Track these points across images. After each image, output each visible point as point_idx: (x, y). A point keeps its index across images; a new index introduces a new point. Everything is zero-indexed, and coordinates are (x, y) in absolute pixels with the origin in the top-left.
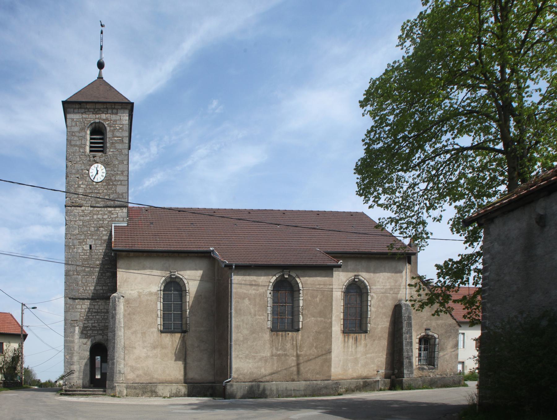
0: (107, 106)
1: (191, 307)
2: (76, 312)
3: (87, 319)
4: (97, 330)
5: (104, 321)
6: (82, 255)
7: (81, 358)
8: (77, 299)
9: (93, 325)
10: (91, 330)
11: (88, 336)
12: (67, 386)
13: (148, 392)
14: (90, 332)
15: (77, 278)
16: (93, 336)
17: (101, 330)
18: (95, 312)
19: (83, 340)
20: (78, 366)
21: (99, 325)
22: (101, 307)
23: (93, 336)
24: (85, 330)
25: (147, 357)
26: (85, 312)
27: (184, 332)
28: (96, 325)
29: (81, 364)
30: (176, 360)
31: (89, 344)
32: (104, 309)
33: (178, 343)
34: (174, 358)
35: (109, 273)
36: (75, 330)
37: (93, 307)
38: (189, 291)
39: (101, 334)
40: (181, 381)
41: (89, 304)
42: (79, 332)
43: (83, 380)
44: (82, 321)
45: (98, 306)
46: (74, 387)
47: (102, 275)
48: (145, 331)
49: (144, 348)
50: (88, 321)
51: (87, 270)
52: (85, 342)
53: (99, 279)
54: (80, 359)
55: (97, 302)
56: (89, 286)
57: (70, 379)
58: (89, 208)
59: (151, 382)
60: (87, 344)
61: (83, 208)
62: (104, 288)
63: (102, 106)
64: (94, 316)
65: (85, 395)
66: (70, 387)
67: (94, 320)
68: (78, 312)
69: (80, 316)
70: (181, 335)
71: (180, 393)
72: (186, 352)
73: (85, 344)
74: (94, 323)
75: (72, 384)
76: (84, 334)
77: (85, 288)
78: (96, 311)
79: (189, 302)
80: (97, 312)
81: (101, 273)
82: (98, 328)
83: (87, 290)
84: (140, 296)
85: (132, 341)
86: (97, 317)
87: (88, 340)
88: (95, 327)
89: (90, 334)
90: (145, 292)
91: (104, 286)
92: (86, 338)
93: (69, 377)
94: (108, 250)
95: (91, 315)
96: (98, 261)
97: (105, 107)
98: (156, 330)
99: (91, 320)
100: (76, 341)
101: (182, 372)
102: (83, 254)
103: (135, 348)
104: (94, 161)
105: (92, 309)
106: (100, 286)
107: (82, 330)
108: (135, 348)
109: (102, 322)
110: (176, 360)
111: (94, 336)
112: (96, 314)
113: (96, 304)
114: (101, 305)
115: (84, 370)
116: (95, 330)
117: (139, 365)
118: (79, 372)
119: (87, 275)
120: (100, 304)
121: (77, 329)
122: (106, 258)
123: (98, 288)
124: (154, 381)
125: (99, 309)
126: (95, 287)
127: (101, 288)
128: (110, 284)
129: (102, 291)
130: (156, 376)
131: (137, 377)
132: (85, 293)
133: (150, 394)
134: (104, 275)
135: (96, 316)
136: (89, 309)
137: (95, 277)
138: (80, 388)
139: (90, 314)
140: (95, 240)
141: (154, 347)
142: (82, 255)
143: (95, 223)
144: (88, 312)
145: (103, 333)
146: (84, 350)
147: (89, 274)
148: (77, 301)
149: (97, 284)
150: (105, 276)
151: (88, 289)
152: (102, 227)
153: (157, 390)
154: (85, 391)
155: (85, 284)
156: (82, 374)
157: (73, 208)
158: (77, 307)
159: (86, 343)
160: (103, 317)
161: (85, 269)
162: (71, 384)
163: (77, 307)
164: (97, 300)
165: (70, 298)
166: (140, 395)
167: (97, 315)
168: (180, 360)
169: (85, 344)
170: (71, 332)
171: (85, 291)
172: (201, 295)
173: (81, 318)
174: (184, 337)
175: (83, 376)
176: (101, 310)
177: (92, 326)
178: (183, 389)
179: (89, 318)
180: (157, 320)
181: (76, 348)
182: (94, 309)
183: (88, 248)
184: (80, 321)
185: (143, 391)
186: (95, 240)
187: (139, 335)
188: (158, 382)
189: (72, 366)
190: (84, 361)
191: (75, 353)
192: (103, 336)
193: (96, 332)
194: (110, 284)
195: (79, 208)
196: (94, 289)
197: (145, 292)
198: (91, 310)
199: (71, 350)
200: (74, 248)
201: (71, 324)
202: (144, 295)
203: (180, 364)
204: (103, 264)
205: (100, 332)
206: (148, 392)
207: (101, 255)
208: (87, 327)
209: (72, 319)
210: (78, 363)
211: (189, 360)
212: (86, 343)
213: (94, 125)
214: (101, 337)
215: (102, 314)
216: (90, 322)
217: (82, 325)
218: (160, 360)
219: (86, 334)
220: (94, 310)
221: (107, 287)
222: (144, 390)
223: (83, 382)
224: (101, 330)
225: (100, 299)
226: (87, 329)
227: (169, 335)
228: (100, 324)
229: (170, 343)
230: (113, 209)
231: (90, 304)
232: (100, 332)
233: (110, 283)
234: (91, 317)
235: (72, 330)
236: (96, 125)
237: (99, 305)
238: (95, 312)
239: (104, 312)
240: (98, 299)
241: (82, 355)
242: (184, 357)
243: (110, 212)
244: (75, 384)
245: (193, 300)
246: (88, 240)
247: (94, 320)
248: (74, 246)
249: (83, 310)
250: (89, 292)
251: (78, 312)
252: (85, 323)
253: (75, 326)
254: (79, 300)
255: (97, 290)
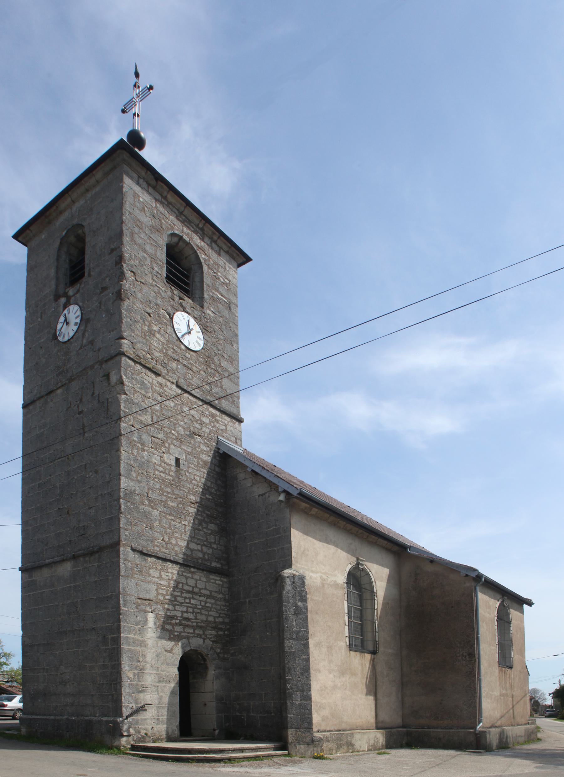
0: (206, 229)
1: (380, 617)
2: (149, 582)
3: (173, 601)
4: (194, 628)
5: (207, 613)
6: (161, 472)
7: (161, 679)
8: (150, 556)
9: (185, 615)
10: (180, 624)
11: (174, 635)
12: (130, 739)
13: (343, 745)
14: (178, 629)
15: (150, 513)
16: (185, 637)
17: (201, 627)
18: (188, 592)
19: (164, 642)
20: (155, 696)
21: (196, 619)
22: (201, 585)
23: (185, 637)
24: (168, 624)
25: (335, 687)
26: (169, 586)
27: (374, 653)
28: (191, 616)
29: (162, 692)
30: (367, 694)
31: (178, 652)
32: (206, 589)
33: (369, 668)
34: (365, 690)
35: (213, 525)
36: (146, 621)
37: (184, 580)
38: (376, 593)
39: (199, 636)
40: (373, 726)
41: (176, 572)
42: (155, 624)
43: (167, 724)
44: (162, 603)
45: (194, 582)
46: (148, 739)
47: (200, 524)
48: (331, 644)
49: (330, 673)
50: (174, 606)
51: (170, 503)
52: (170, 646)
53: (194, 529)
54: (159, 682)
55: (191, 572)
56: (176, 538)
57: (137, 722)
58: (174, 387)
59: (340, 728)
60: (174, 651)
61: (160, 379)
62: (205, 549)
63: (197, 222)
64: (185, 598)
65: (256, 758)
66: (139, 740)
67: (187, 607)
68: (153, 583)
69: (158, 594)
70: (371, 656)
71: (379, 744)
72: (376, 682)
73: (170, 651)
74: (187, 612)
75: (143, 732)
76: (167, 630)
77: (166, 539)
78: (191, 589)
79: (377, 609)
80: (192, 592)
81: (199, 520)
82: (195, 624)
83: (171, 543)
84: (323, 585)
85: (315, 660)
86: (193, 601)
87: (176, 645)
88: (188, 619)
89: (180, 633)
90: (329, 580)
91: (205, 545)
92: (170, 639)
93: (134, 717)
94: (212, 483)
95: (181, 596)
96: (194, 495)
97: (201, 226)
98: (344, 644)
99: (181, 604)
100: (150, 643)
101: (373, 713)
102: (161, 469)
103: (320, 672)
104: (181, 305)
105: (183, 583)
106: (198, 544)
107: (164, 622)
108: (320, 672)
109: (201, 614)
110: (367, 694)
111: (188, 638)
112: (190, 595)
113: (190, 575)
114: (200, 580)
115: (170, 703)
116: (187, 626)
117: (324, 701)
118: (159, 708)
119: (170, 514)
120: (196, 577)
121: (151, 617)
122: (207, 496)
123: (193, 546)
124: (344, 726)
125: (196, 587)
126: (188, 543)
127: (199, 547)
128: (215, 546)
129: (201, 555)
130: (345, 719)
131: (323, 720)
132: (167, 548)
133: (345, 748)
134: (204, 525)
135: (190, 598)
136: (177, 582)
137: (188, 523)
138: (162, 740)
139: (179, 594)
140: (188, 453)
141: (343, 673)
142: (161, 472)
143: (186, 420)
144: (176, 587)
145: (204, 634)
146: (168, 664)
147: (175, 514)
148: (150, 559)
149: (192, 538)
150: (207, 528)
151: (174, 541)
152: (200, 436)
153: (354, 742)
154: (242, 750)
155: (168, 530)
156: (166, 713)
157: (139, 367)
158: (151, 572)
159: (172, 649)
160: (203, 604)
161: (166, 501)
162: (139, 732)
163: (151, 572)
164: (192, 570)
165: (134, 550)
166: (334, 751)
167: (193, 598)
168: (371, 695)
169: (170, 651)
170: (137, 624)
171: (167, 544)
172: (388, 603)
173: (161, 597)
174: (374, 659)
175: (167, 715)
176: (200, 589)
177: (182, 617)
178: (379, 737)
179: (176, 600)
180: (344, 628)
181: (150, 657)
182: (187, 584)
183: (173, 462)
184: (156, 603)
185: (337, 744)
186: (188, 453)
187: (324, 650)
188: (348, 728)
189: (141, 696)
190: (168, 685)
191: (148, 666)
192: (204, 639)
193: (191, 631)
194: (215, 546)
195: (153, 376)
196: (187, 547)
197: (329, 580)
198: (180, 585)
199: (139, 661)
200: (144, 450)
201: (138, 605)
202: (328, 585)
203: (371, 698)
204: (202, 506)
205: (198, 632)
206: (343, 745)
207: (197, 485)
208: (172, 618)
209: (141, 596)
210: (155, 689)
211: (379, 696)
212: (172, 649)
213: (175, 240)
214: (200, 641)
215: (202, 598)
216: (177, 608)
217: (162, 613)
218: (350, 693)
219: (171, 632)
220: (186, 587)
221: (211, 550)
222: (339, 742)
223: (167, 728)
224: (201, 627)
225: (198, 569)
226: (173, 621)
227: (358, 653)
228: (199, 617)
229: (360, 668)
230: (218, 413)
231: (178, 574)
232: (197, 632)
233: (215, 543)
234: (179, 599)
235: (139, 619)
236: (181, 243)
237: (196, 580)
238: (188, 592)
239: (204, 595)
240: (194, 567)
241: (164, 673)
242: (374, 690)
243: (213, 416)
244: (149, 734)
245: (382, 609)
246: (172, 446)
247: (187, 607)
248: (142, 444)
249: (163, 582)
250: (176, 549)
251: (153, 583)
252: (168, 609)
253: (146, 612)
254: (154, 559)
255: (192, 550)
